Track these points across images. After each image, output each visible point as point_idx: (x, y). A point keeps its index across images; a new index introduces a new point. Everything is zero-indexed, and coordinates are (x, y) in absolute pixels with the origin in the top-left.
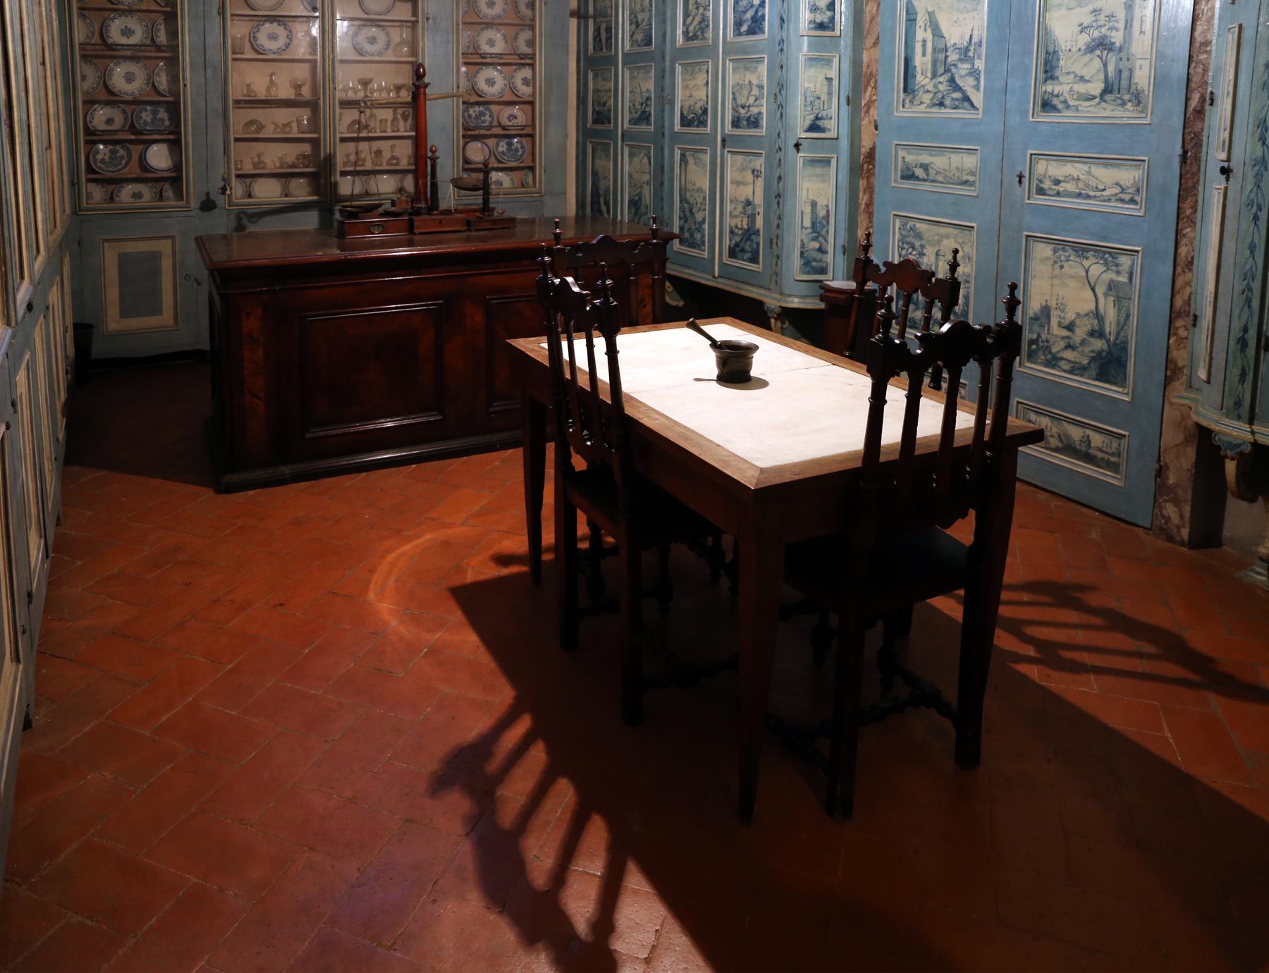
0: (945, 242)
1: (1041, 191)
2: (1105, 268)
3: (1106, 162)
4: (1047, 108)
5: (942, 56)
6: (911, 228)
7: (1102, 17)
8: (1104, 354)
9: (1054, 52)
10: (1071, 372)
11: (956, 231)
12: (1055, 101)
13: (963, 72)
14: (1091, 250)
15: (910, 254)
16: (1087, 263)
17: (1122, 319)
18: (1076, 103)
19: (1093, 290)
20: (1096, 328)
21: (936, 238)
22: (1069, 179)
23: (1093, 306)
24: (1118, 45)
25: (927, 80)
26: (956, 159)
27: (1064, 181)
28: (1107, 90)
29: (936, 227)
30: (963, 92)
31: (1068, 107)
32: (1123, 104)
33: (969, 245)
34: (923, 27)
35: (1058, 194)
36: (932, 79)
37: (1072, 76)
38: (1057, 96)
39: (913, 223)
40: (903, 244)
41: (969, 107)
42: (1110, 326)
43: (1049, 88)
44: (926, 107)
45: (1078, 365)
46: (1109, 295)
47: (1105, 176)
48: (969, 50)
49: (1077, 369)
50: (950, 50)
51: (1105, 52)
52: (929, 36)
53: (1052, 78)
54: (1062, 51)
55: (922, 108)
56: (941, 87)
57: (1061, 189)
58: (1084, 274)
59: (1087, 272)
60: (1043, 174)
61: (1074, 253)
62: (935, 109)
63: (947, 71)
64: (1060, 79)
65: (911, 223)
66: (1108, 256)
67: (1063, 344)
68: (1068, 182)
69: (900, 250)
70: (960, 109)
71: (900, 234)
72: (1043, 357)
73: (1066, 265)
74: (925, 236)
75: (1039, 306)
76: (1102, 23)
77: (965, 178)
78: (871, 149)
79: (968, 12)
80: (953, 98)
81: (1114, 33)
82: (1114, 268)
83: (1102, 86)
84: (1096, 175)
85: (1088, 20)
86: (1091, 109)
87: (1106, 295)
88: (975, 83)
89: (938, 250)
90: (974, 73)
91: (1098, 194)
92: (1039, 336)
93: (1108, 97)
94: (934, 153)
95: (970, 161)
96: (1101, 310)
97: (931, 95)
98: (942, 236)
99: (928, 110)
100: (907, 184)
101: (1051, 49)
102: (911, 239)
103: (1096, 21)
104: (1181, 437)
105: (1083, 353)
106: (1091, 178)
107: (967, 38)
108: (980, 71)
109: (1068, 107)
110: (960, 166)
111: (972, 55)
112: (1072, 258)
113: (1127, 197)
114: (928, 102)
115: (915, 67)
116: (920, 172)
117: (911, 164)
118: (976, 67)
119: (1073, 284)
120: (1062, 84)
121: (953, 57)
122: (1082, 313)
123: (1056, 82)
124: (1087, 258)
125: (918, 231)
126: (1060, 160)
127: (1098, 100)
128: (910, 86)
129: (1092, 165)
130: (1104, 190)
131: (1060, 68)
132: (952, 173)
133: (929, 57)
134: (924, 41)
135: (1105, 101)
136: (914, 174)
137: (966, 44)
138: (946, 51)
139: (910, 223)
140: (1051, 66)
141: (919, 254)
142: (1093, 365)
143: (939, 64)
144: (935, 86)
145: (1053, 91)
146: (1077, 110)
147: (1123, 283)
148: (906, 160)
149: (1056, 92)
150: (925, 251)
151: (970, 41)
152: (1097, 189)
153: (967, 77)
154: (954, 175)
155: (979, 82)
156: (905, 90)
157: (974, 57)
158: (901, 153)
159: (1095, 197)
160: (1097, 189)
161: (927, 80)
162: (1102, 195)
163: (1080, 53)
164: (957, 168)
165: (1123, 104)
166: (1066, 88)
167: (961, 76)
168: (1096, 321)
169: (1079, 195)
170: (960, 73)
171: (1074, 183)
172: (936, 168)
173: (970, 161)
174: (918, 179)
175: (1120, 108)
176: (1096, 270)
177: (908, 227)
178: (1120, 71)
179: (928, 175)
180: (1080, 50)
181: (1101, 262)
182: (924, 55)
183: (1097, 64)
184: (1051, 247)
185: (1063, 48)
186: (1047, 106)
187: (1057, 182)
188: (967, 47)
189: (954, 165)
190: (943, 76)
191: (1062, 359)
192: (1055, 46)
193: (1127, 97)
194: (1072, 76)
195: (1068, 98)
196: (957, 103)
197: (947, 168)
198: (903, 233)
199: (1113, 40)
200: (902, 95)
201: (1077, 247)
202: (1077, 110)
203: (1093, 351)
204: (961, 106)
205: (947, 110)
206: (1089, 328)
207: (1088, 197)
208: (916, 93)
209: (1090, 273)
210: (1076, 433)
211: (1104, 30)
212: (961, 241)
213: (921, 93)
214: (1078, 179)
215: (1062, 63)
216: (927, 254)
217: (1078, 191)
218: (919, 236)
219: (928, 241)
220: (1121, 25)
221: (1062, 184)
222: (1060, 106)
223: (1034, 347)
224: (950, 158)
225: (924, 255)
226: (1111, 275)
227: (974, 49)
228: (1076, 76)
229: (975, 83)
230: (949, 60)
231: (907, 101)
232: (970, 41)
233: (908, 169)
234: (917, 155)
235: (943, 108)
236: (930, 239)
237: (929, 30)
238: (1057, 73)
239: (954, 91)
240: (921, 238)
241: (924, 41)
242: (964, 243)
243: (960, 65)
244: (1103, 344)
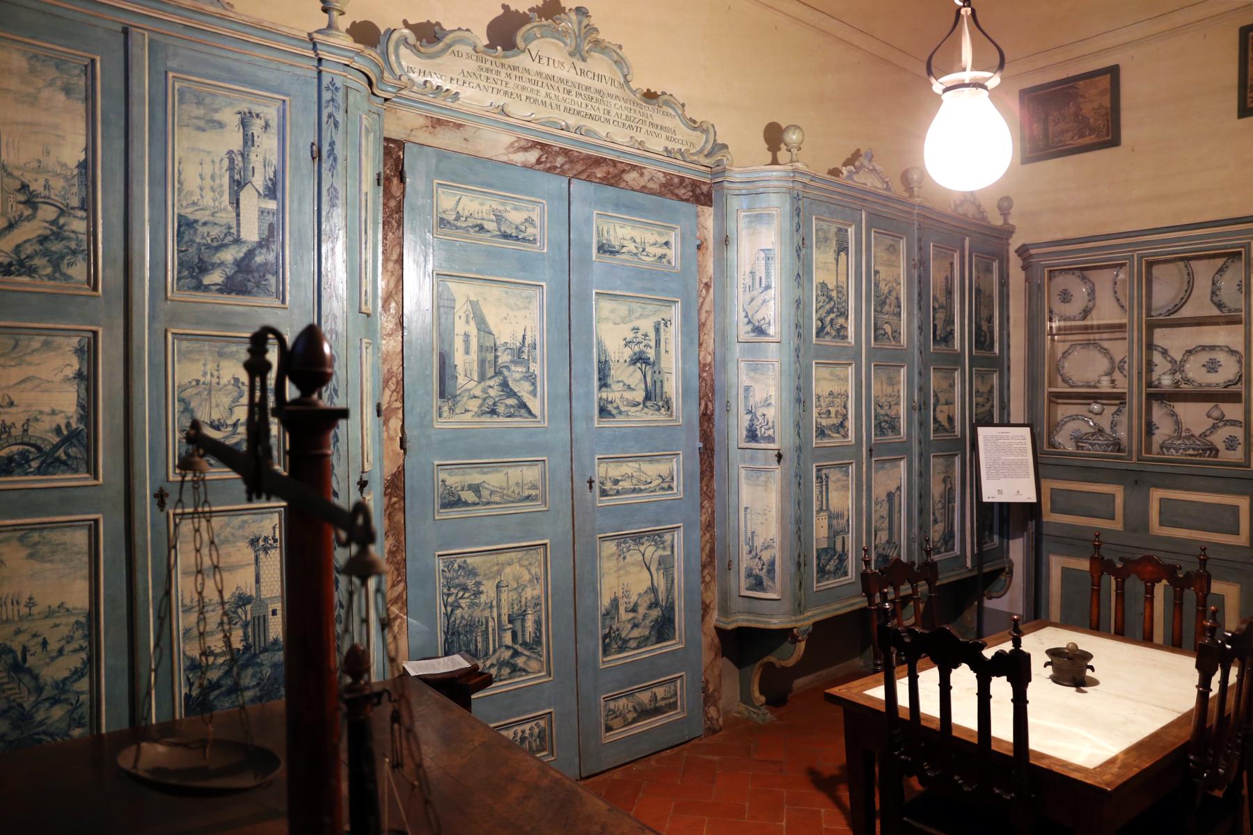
0: (508, 570)
1: (604, 493)
3: (651, 459)
5: (490, 356)
6: (459, 566)
7: (639, 335)
10: (638, 647)
11: (520, 554)
12: (610, 407)
13: (518, 376)
15: (462, 598)
16: (642, 548)
17: (669, 585)
19: (649, 569)
21: (496, 568)
23: (649, 583)
24: (652, 360)
25: (473, 384)
26: (515, 474)
28: (648, 397)
29: (495, 556)
30: (519, 398)
31: (620, 413)
32: (659, 410)
33: (537, 564)
34: (464, 318)
35: (618, 493)
36: (479, 383)
38: (611, 402)
39: (463, 559)
40: (449, 590)
41: (527, 415)
42: (662, 595)
44: (473, 416)
45: (642, 639)
47: (652, 470)
48: (523, 352)
49: (643, 642)
50: (501, 349)
51: (644, 365)
52: (472, 329)
55: (468, 416)
56: (492, 393)
57: (620, 488)
58: (641, 558)
59: (643, 555)
60: (604, 476)
61: (633, 542)
62: (486, 418)
63: (498, 373)
65: (460, 561)
66: (656, 537)
67: (629, 626)
68: (625, 480)
69: (445, 598)
70: (516, 416)
71: (445, 577)
72: (616, 646)
73: (627, 555)
74: (481, 571)
75: (609, 601)
76: (640, 340)
77: (526, 493)
78: (394, 475)
79: (519, 309)
80: (507, 405)
81: (648, 350)
82: (662, 546)
83: (643, 394)
85: (630, 336)
86: (638, 414)
87: (658, 570)
88: (531, 388)
89: (499, 582)
90: (530, 378)
92: (611, 628)
93: (649, 404)
94: (486, 470)
95: (531, 474)
96: (656, 584)
97: (479, 402)
98: (502, 564)
99: (477, 419)
100: (454, 513)
101: (603, 359)
102: (462, 580)
103: (636, 337)
104: (713, 655)
105: (645, 627)
107: (520, 339)
108: (536, 376)
109: (620, 413)
110: (520, 481)
111: (526, 358)
112: (632, 548)
113: (666, 485)
114: (475, 409)
115: (456, 366)
116: (468, 496)
117: (456, 488)
118: (531, 370)
119: (633, 569)
120: (614, 392)
121: (504, 358)
123: (609, 390)
124: (643, 544)
125: (470, 568)
126: (618, 462)
127: (641, 406)
128: (448, 390)
132: (511, 490)
133: (474, 355)
134: (467, 336)
135: (647, 407)
136: (460, 499)
137: (518, 344)
138: (496, 350)
139: (458, 560)
141: (474, 594)
143: (487, 365)
144: (484, 391)
147: (668, 555)
148: (447, 483)
149: (610, 399)
150: (482, 588)
151: (524, 342)
153: (522, 382)
154: (514, 492)
155: (536, 387)
156: (442, 394)
157: (529, 360)
158: (443, 475)
161: (473, 384)
164: (517, 484)
165: (659, 410)
166: (618, 395)
167: (515, 380)
169: (634, 491)
170: (514, 377)
172: (491, 488)
173: (531, 474)
174: (466, 504)
175: (657, 413)
176: (650, 550)
177: (456, 566)
178: (655, 382)
179: (480, 497)
180: (625, 361)
181: (653, 543)
182: (467, 352)
183: (639, 375)
184: (615, 542)
185: (613, 358)
188: (520, 349)
189: (512, 482)
190: (494, 380)
191: (630, 639)
193: (661, 404)
196: (512, 410)
197: (505, 485)
198: (448, 575)
199: (649, 356)
200: (436, 401)
203: (652, 621)
204: (517, 413)
205: (501, 419)
207: (640, 490)
208: (458, 398)
210: (645, 697)
211: (642, 346)
212: (527, 563)
213: (465, 399)
215: (612, 372)
216: (485, 591)
217: (632, 487)
218: (472, 573)
219: (485, 575)
220: (653, 344)
221: (620, 483)
222: (614, 412)
223: (607, 640)
224: (507, 473)
225: (481, 593)
226: (661, 552)
227: (528, 352)
229: (531, 388)
230: (500, 361)
231: (446, 409)
232: (524, 342)
233: (451, 494)
234: (464, 475)
235: (495, 416)
236: (487, 572)
237: (472, 323)
238: (610, 381)
239: (508, 397)
240: (476, 575)
241: (467, 336)
242: (530, 564)
243: (513, 368)
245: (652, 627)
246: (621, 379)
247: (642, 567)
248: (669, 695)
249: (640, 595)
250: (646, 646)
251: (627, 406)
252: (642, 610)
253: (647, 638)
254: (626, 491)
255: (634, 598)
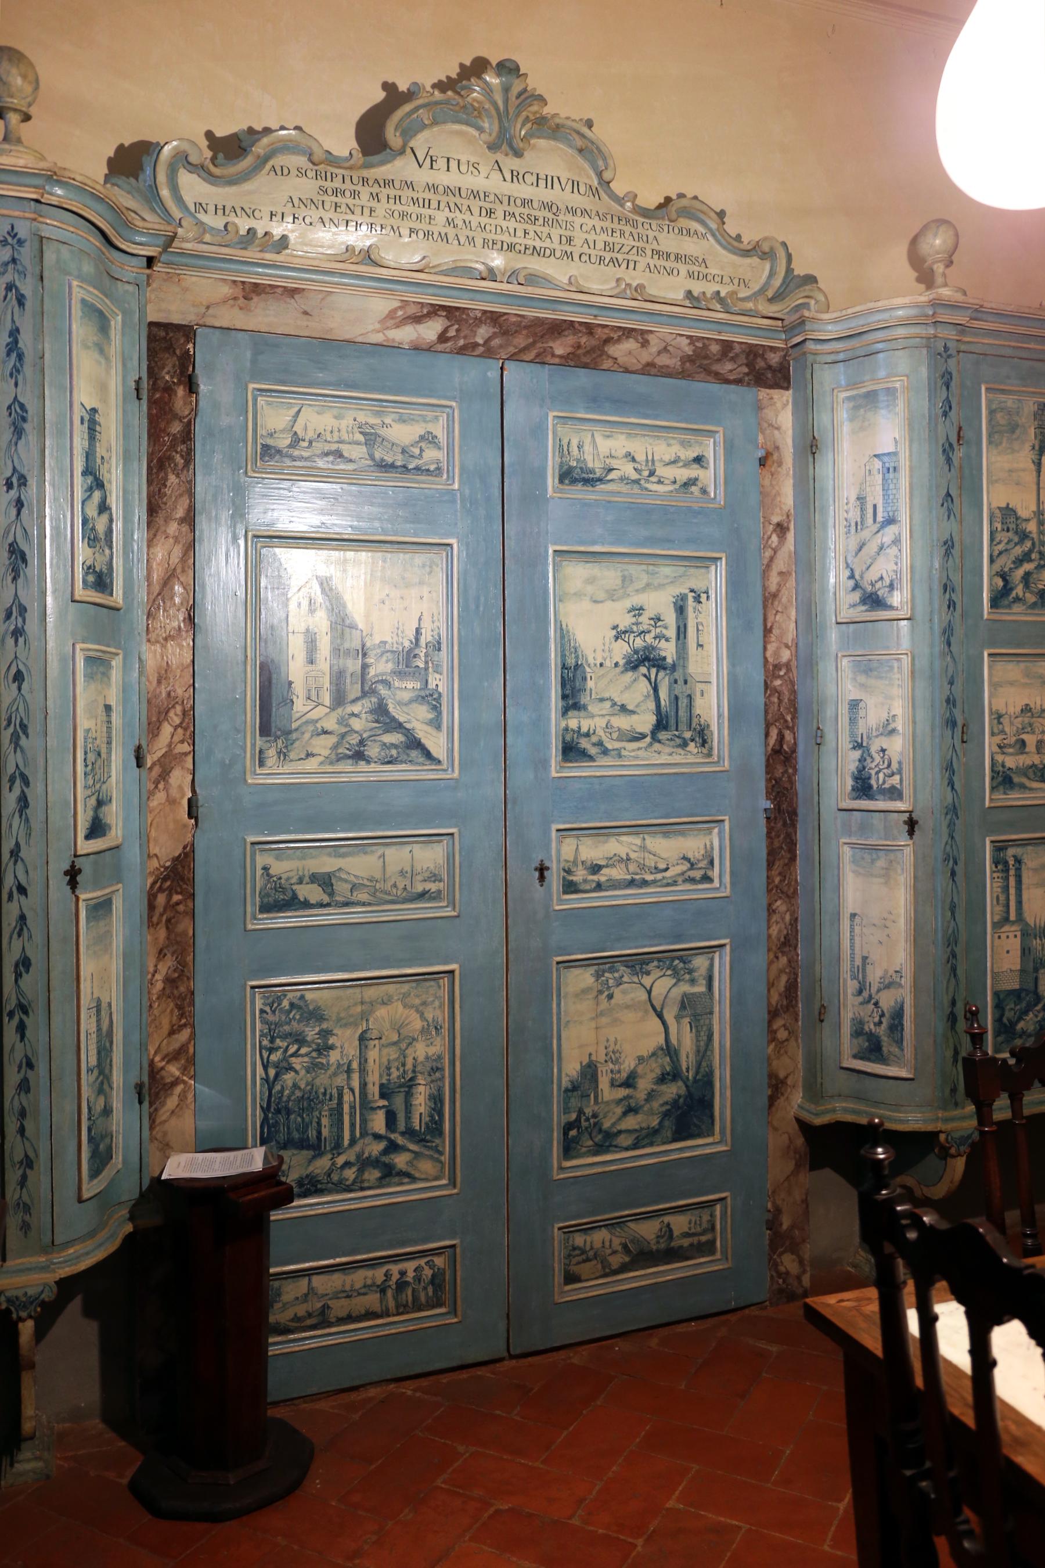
2: (674, 981)
4: (571, 754)
8: (681, 1100)
9: (577, 666)
12: (584, 743)
14: (652, 960)
16: (647, 981)
18: (617, 745)
19: (660, 1016)
20: (668, 1069)
22: (614, 861)
27: (607, 866)
31: (605, 752)
37: (608, 704)
38: (587, 735)
43: (573, 724)
46: (682, 1017)
53: (577, 706)
54: (589, 665)
57: (603, 879)
59: (649, 992)
61: (628, 970)
64: (590, 708)
68: (613, 866)
84: (653, 850)
87: (678, 1018)
91: (659, 876)
106: (647, 854)
109: (605, 752)
112: (626, 979)
119: (629, 1016)
120: (593, 716)
122: (645, 1054)
123: (582, 713)
124: (648, 973)
129: (646, 836)
130: (667, 869)
131: (588, 692)
140: (573, 689)
142: (667, 1123)
145: (579, 728)
146: (620, 756)
149: (584, 730)
152: (657, 870)
159: (654, 882)
160: (657, 870)
162: (664, 878)
163: (618, 670)
166: (599, 723)
168: (668, 1059)
169: (631, 883)
171: (623, 866)
176: (662, 985)
181: (669, 972)
186: (571, 751)
187: (596, 869)
192: (577, 657)
194: (608, 704)
195: (604, 738)
201: (631, 961)
202: (620, 756)
206: (658, 1071)
207: (645, 883)
209: (653, 993)
214: (629, 859)
215: (590, 684)
217: (629, 877)
221: (604, 871)
222: (593, 751)
228: (614, 704)
238: (584, 699)
244: (679, 1087)
245: (666, 1115)
246: (606, 695)
247: (646, 1011)
248: (699, 1229)
249: (641, 1059)
250: (651, 1144)
251: (619, 739)
252: (644, 1085)
253: (656, 1132)
254: (615, 885)
255: (628, 1064)
